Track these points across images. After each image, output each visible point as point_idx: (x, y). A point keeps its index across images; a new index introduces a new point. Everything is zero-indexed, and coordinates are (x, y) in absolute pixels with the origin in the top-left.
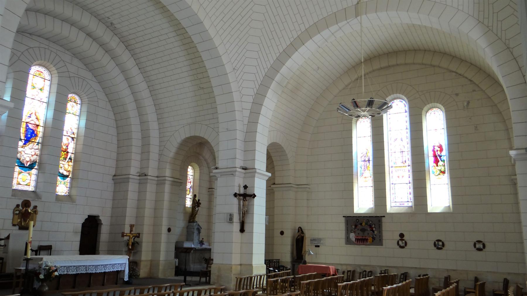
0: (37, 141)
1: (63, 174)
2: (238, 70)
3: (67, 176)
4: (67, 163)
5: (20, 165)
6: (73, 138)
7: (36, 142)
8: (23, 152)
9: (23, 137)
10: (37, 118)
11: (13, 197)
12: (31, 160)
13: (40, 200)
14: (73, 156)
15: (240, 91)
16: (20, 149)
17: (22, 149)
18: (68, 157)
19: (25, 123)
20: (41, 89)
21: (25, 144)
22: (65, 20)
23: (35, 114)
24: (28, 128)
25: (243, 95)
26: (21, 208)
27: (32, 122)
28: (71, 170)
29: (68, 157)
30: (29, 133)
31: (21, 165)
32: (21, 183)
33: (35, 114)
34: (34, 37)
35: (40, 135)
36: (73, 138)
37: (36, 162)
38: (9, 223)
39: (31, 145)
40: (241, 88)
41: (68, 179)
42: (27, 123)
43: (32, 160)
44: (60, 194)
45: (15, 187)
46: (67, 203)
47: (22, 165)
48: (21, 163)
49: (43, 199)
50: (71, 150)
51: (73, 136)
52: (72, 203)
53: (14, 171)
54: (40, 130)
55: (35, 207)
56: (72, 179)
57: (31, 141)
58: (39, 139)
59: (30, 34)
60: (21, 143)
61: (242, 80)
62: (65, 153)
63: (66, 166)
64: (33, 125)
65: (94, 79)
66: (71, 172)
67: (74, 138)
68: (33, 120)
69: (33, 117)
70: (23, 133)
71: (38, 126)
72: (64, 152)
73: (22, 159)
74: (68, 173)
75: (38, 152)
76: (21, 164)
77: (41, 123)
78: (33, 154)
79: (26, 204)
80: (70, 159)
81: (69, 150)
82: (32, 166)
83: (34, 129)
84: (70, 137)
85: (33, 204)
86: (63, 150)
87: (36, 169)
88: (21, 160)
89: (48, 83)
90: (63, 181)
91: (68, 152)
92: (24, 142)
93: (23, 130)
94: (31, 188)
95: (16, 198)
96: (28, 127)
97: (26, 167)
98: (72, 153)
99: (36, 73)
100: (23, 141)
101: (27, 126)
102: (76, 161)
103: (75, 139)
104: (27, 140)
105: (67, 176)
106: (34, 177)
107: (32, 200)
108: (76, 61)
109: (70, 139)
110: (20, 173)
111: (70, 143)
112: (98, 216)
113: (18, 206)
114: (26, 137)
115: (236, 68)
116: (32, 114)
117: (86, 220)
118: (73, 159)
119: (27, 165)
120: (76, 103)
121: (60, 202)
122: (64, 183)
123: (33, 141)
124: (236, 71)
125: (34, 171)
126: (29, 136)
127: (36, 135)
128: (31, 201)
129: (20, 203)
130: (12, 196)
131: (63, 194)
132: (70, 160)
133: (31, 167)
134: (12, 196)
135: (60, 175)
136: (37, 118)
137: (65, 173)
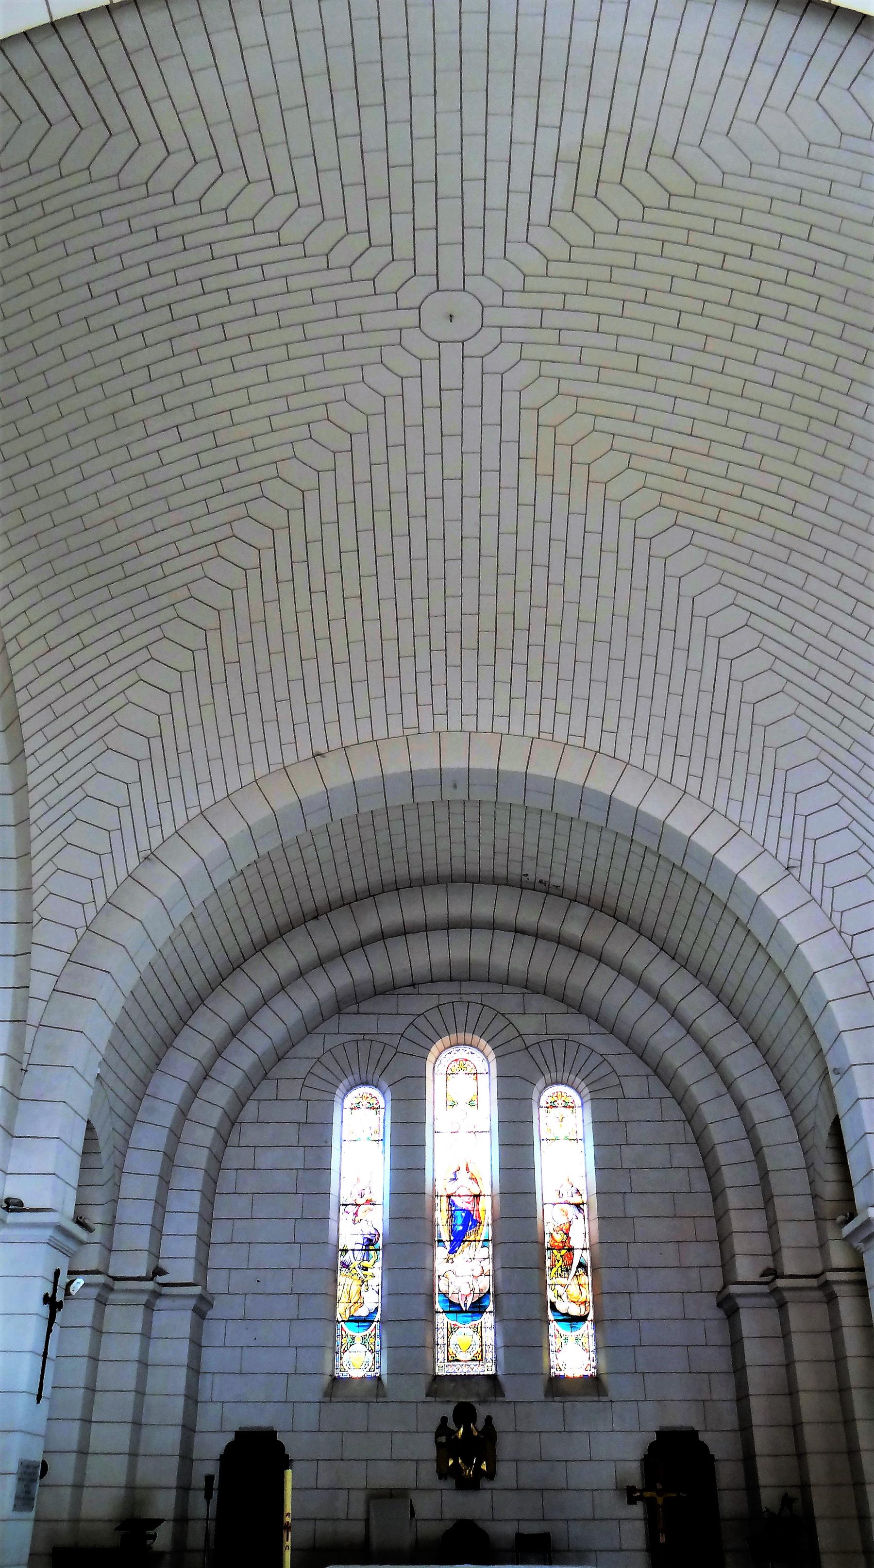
0: (482, 1239)
1: (567, 1314)
2: (801, 866)
3: (583, 1319)
4: (575, 1278)
5: (448, 1310)
6: (578, 1206)
7: (479, 1241)
8: (449, 1274)
9: (445, 1236)
10: (474, 1179)
11: (429, 1399)
12: (473, 1290)
13: (500, 1399)
14: (587, 1256)
15: (837, 924)
16: (440, 1267)
17: (449, 1266)
18: (575, 1263)
19: (444, 1199)
20: (471, 1103)
21: (452, 1251)
22: (450, 925)
23: (467, 1169)
24: (453, 1208)
25: (853, 936)
26: (451, 1425)
27: (462, 1192)
28: (590, 1298)
29: (575, 1263)
30: (460, 1221)
31: (452, 1309)
32: (459, 1357)
33: (467, 1169)
34: (423, 989)
35: (486, 1217)
36: (578, 1206)
37: (489, 1292)
38: (428, 1473)
39: (466, 1251)
40: (836, 917)
41: (587, 1328)
42: (449, 1196)
43: (477, 1291)
44: (571, 1375)
45: (444, 1369)
46: (581, 1398)
47: (454, 1308)
48: (451, 1302)
49: (510, 1396)
50: (578, 1240)
51: (577, 1199)
52: (596, 1399)
53: (434, 1329)
54: (485, 1204)
55: (489, 1419)
56: (596, 1322)
57: (466, 1241)
58: (485, 1231)
59: (413, 985)
60: (441, 1252)
61: (828, 892)
62: (563, 1252)
63: (574, 1290)
64: (466, 1198)
65: (595, 1027)
66: (591, 1304)
67: (583, 1204)
68: (464, 1186)
69: (463, 1176)
70: (444, 1223)
71: (477, 1196)
72: (559, 1250)
73: (451, 1293)
74: (583, 1307)
75: (488, 1266)
76: (450, 1307)
77: (486, 1190)
78: (477, 1272)
79: (465, 1413)
80: (581, 1265)
81: (573, 1243)
82: (480, 1307)
83: (470, 1207)
84: (569, 1204)
85: (482, 1412)
86: (557, 1244)
87: (490, 1312)
88: (449, 1296)
89: (483, 1079)
90: (572, 1335)
91: (571, 1249)
92: (449, 1248)
93: (441, 1216)
94: (488, 1369)
95: (438, 1399)
96: (454, 1204)
97: (466, 1312)
98: (583, 1249)
99: (451, 1066)
100: (447, 1244)
101: (452, 1204)
102: (595, 1269)
103: (585, 1207)
104: (458, 1240)
105: (583, 1319)
106: (489, 1336)
107: (480, 1402)
108: (536, 1002)
109: (572, 1210)
110: (451, 1331)
111: (574, 1221)
112: (692, 1434)
113: (444, 1420)
114: (452, 1231)
115: (792, 863)
116: (459, 1170)
117: (652, 1447)
118: (589, 1265)
119: (466, 1305)
120: (570, 1107)
121: (556, 1399)
122: (577, 1339)
123: (472, 1238)
124: (796, 872)
125: (488, 1319)
126: (461, 1228)
127: (477, 1223)
128: (477, 1406)
129: (448, 1411)
130: (427, 1395)
131: (579, 1373)
132: (581, 1271)
133: (477, 1308)
134: (427, 1395)
135: (561, 1318)
136: (474, 1179)
137: (575, 1311)
